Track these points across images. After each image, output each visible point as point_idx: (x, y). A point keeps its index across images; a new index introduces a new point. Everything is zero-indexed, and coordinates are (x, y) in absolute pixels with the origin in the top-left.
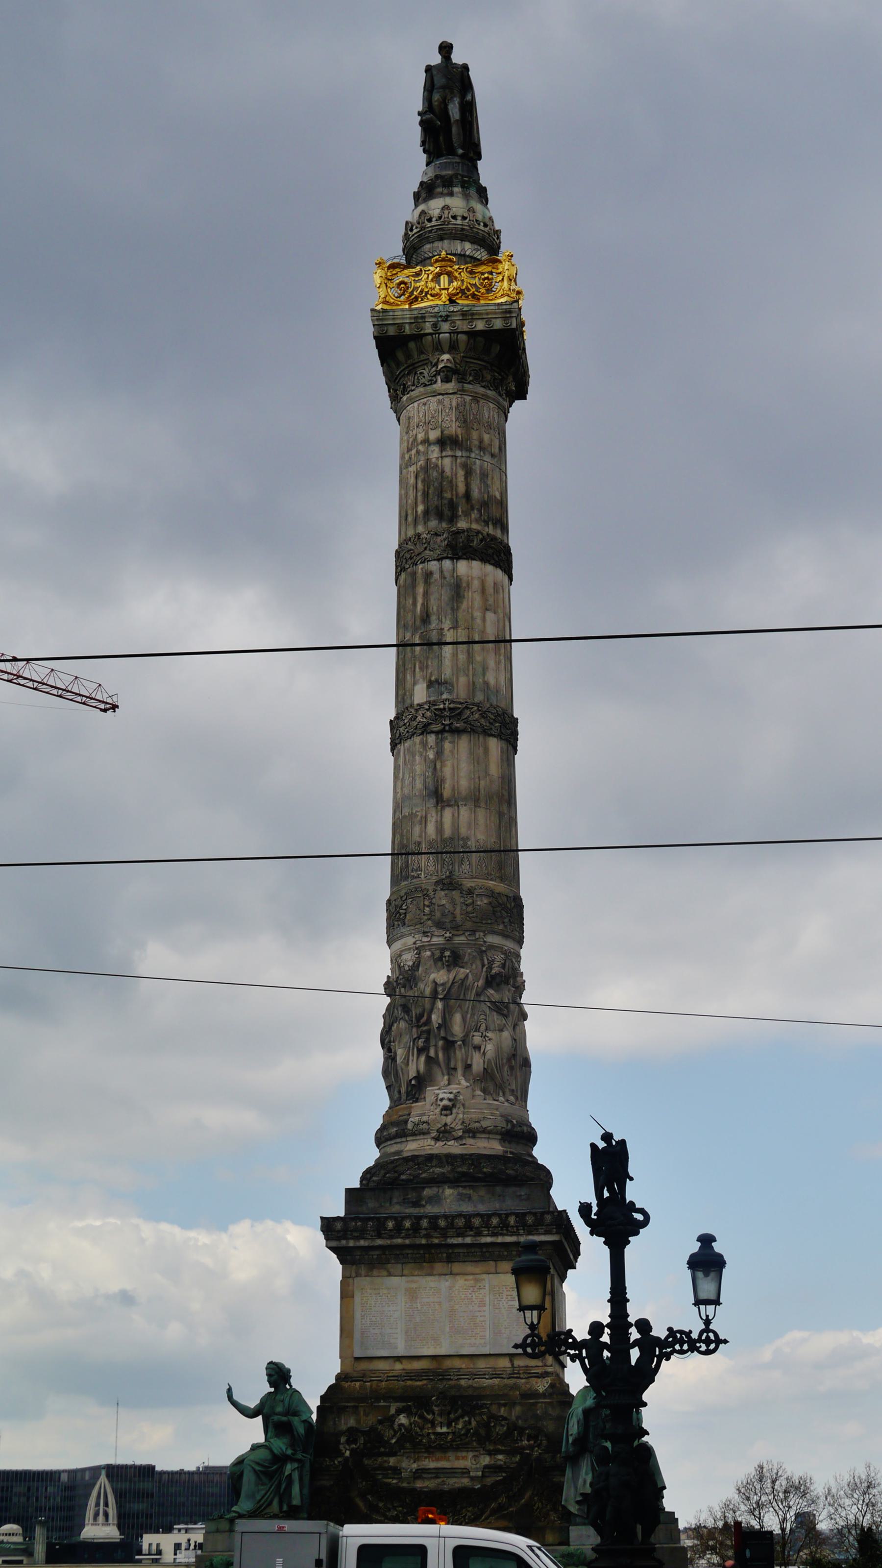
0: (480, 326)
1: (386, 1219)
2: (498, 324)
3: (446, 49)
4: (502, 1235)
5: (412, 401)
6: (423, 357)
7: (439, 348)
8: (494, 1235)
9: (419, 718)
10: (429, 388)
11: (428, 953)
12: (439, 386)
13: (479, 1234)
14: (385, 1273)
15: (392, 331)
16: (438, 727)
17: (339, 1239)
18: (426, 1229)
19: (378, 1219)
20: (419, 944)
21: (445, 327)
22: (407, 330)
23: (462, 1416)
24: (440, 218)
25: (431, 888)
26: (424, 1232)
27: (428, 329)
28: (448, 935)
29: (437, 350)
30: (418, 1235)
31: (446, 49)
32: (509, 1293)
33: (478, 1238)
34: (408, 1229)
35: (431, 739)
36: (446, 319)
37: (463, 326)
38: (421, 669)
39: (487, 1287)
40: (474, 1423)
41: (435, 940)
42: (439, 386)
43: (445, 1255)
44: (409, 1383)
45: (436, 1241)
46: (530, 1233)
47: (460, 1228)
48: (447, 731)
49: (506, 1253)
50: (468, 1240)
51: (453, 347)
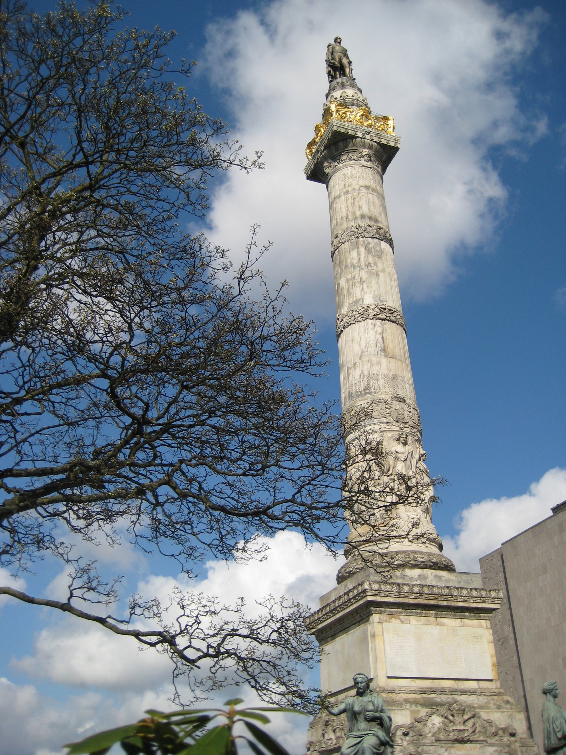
0: (384, 142)
1: (404, 584)
2: (392, 144)
3: (338, 40)
5: (346, 166)
6: (354, 148)
7: (364, 146)
8: (465, 601)
9: (370, 311)
10: (358, 162)
11: (390, 435)
12: (363, 162)
14: (399, 621)
15: (342, 130)
16: (384, 317)
17: (375, 595)
19: (399, 585)
20: (383, 429)
21: (368, 137)
22: (350, 132)
24: (353, 96)
25: (389, 400)
26: (426, 596)
27: (360, 135)
28: (401, 426)
29: (363, 146)
31: (338, 40)
35: (378, 322)
36: (368, 133)
37: (376, 139)
38: (368, 287)
41: (393, 428)
42: (363, 162)
44: (425, 696)
46: (484, 602)
48: (388, 320)
51: (370, 147)
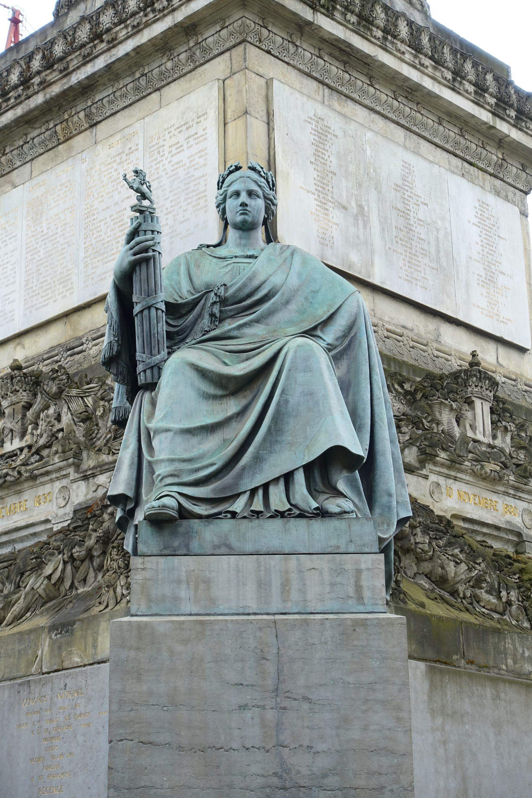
4: (147, 25)
8: (138, 29)
13: (114, 43)
18: (38, 73)
23: (47, 407)
26: (36, 80)
30: (30, 92)
32: (174, 140)
33: (114, 51)
34: (15, 87)
39: (141, 147)
40: (66, 418)
43: (82, 115)
45: (56, 89)
47: (83, 46)
49: (169, 65)
50: (100, 63)
